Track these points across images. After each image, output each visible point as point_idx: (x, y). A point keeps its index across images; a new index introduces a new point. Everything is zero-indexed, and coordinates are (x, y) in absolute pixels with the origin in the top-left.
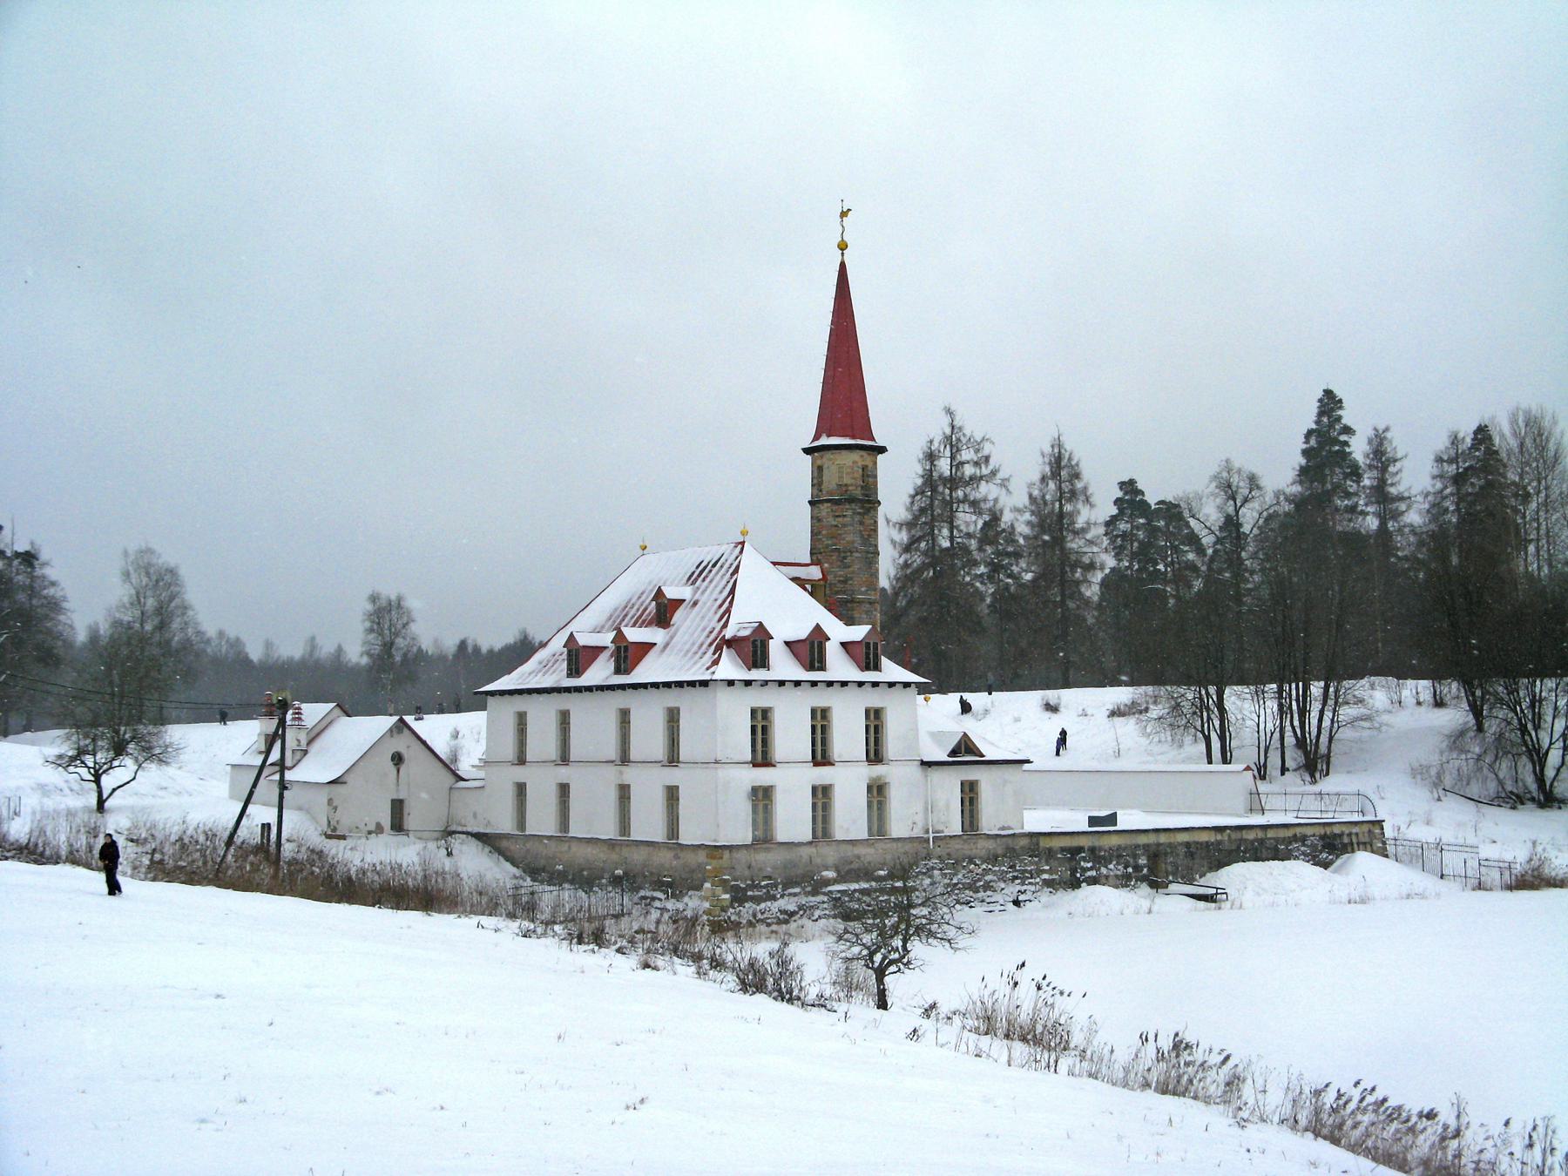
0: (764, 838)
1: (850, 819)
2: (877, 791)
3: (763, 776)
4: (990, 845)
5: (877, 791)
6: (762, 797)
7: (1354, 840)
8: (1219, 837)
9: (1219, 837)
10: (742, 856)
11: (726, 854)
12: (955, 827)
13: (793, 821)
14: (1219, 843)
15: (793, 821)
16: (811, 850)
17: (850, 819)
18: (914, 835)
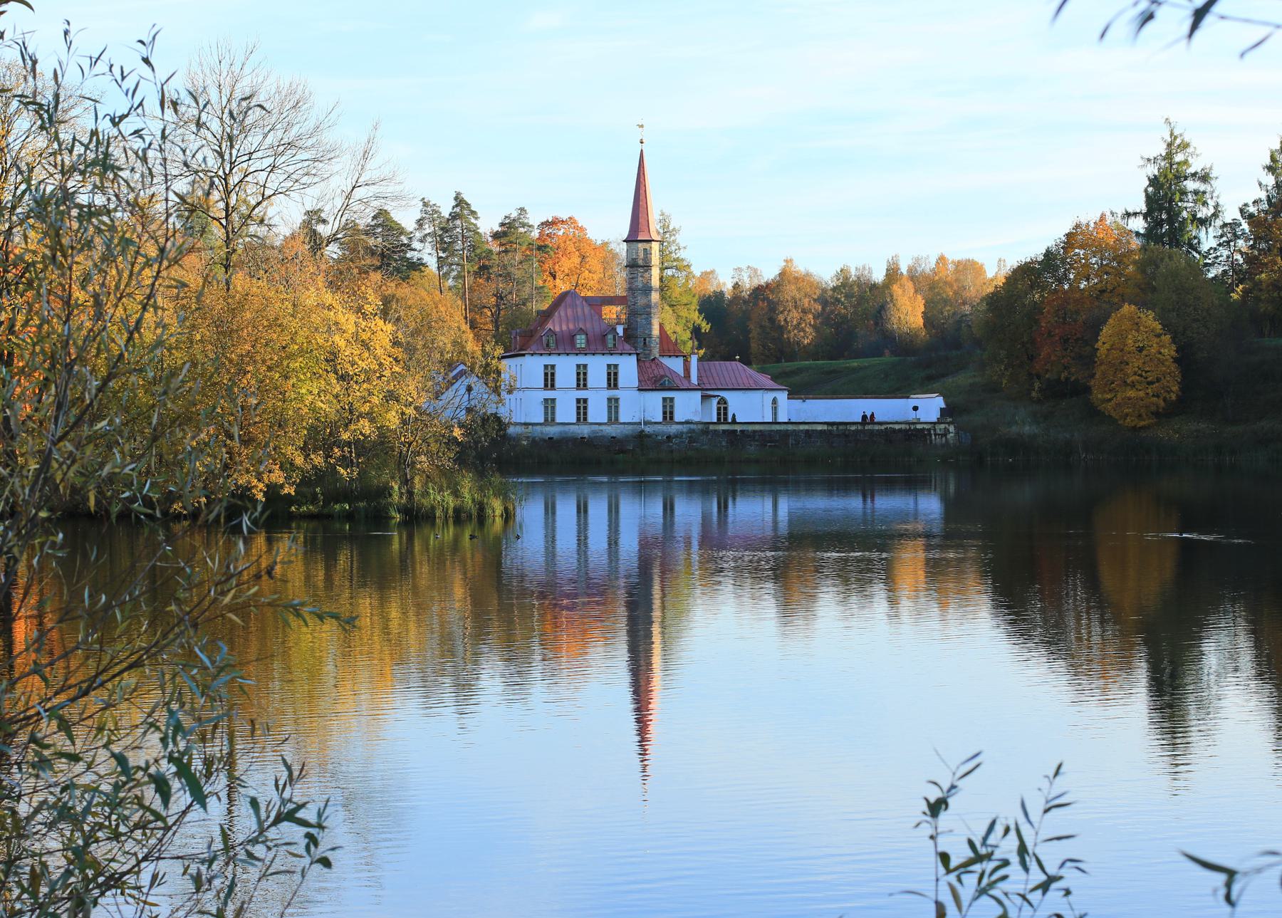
0: (550, 419)
1: (597, 412)
2: (613, 404)
3: (550, 394)
4: (680, 427)
5: (613, 404)
6: (549, 405)
7: (932, 432)
8: (830, 428)
9: (830, 428)
10: (538, 428)
11: (530, 427)
12: (660, 419)
13: (565, 413)
14: (830, 431)
15: (565, 413)
16: (577, 427)
17: (597, 412)
18: (634, 421)
